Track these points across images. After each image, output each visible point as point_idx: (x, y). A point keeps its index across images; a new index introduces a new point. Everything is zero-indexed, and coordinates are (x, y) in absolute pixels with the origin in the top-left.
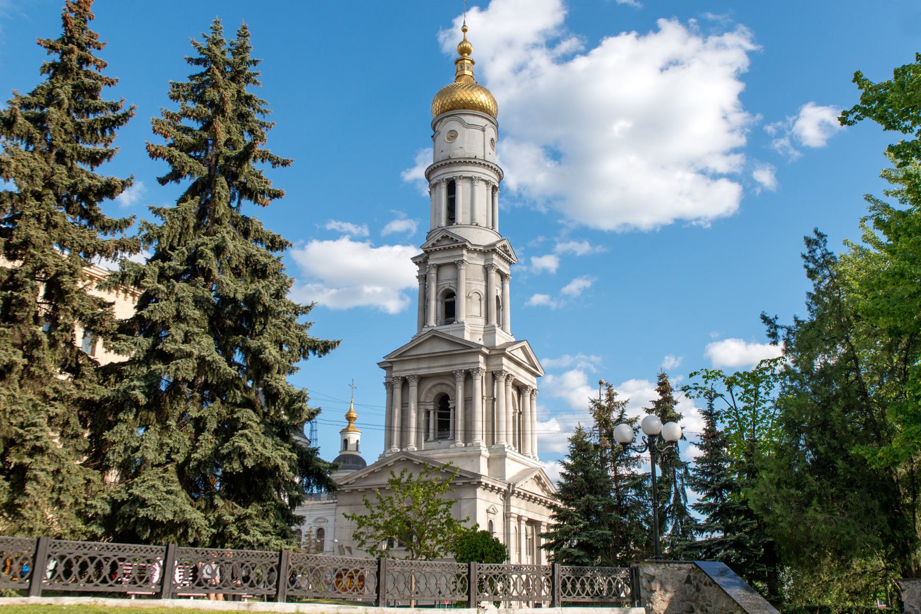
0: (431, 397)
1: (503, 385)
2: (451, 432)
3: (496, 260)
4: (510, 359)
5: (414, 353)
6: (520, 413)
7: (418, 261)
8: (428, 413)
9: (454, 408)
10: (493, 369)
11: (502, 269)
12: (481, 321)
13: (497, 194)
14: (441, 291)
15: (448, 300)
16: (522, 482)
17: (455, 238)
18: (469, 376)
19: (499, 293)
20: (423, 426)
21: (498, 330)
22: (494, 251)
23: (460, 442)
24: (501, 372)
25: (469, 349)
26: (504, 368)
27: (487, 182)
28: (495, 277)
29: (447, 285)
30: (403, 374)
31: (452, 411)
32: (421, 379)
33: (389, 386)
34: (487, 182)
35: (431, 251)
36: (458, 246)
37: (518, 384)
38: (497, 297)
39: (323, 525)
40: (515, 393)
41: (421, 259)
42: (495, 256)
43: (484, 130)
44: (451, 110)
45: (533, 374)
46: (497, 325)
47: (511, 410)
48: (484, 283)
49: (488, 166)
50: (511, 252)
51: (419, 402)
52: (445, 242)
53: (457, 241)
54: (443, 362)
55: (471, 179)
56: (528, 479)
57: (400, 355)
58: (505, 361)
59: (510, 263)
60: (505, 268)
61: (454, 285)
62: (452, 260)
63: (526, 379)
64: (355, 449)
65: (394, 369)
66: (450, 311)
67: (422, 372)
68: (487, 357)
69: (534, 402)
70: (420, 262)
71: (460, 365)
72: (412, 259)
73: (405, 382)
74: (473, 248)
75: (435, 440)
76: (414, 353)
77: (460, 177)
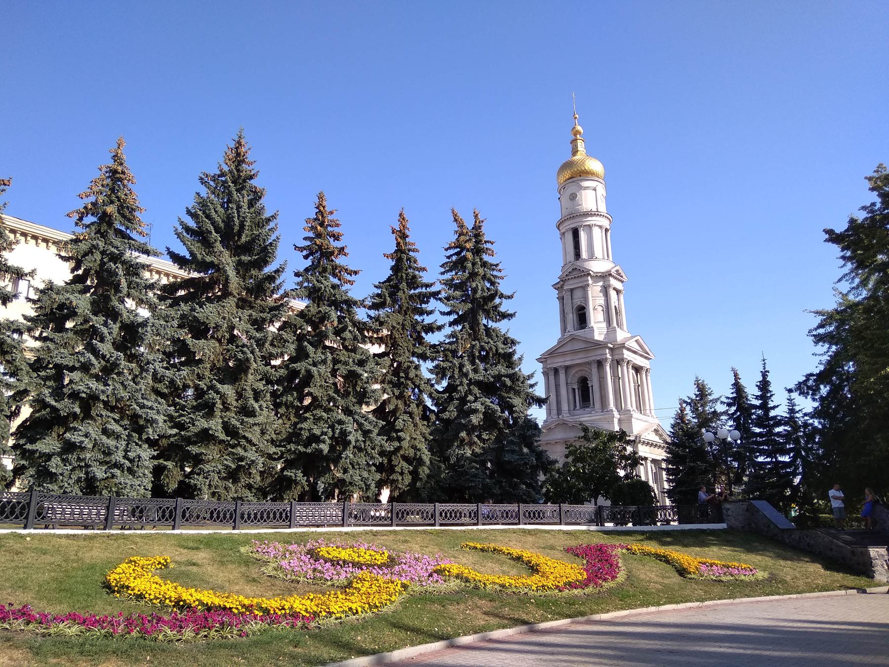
0: (575, 380)
1: (625, 368)
2: (591, 403)
3: (613, 282)
4: (629, 350)
5: (560, 351)
6: (639, 386)
7: (557, 286)
8: (574, 390)
9: (592, 386)
10: (617, 357)
12: (604, 325)
13: (609, 234)
14: (575, 307)
15: (580, 312)
16: (646, 434)
18: (600, 364)
19: (617, 304)
22: (610, 275)
24: (623, 360)
25: (599, 345)
26: (625, 356)
27: (601, 227)
28: (613, 294)
29: (578, 302)
30: (555, 366)
31: (590, 388)
32: (567, 368)
34: (601, 227)
36: (584, 275)
37: (636, 366)
38: (615, 306)
41: (559, 285)
42: (611, 278)
43: (595, 189)
44: (571, 178)
45: (646, 358)
46: (617, 327)
47: (632, 385)
49: (601, 215)
50: (623, 274)
54: (581, 355)
55: (590, 227)
56: (650, 432)
58: (625, 351)
59: (622, 282)
60: (619, 286)
62: (581, 285)
63: (642, 362)
66: (582, 318)
68: (611, 349)
69: (649, 378)
71: (594, 356)
73: (556, 371)
76: (560, 351)
77: (581, 225)
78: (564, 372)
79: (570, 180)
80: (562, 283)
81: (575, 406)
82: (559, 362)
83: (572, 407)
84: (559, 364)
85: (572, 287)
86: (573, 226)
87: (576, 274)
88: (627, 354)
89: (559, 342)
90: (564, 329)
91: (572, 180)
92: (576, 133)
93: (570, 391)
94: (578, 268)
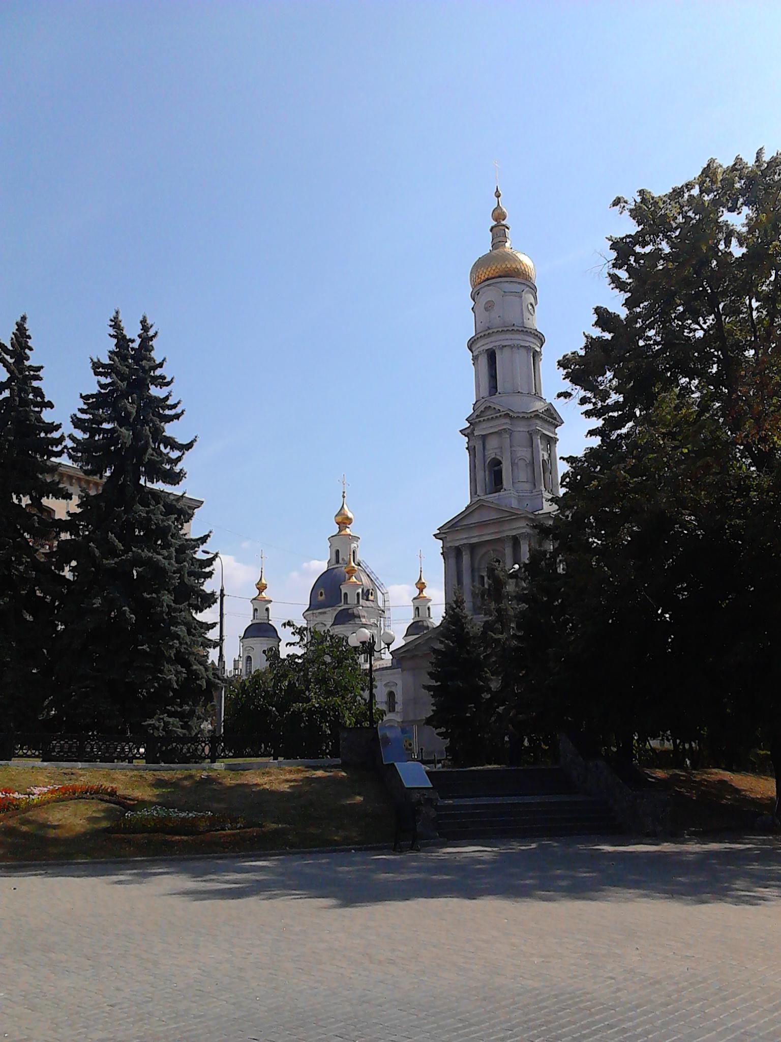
3: (539, 426)
7: (466, 432)
14: (488, 462)
15: (496, 468)
17: (497, 408)
18: (516, 541)
19: (546, 457)
25: (514, 516)
27: (528, 348)
28: (539, 443)
32: (473, 548)
35: (476, 422)
36: (500, 416)
38: (543, 460)
39: (393, 689)
48: (530, 450)
52: (488, 413)
53: (499, 410)
54: (493, 529)
61: (499, 454)
62: (496, 430)
64: (427, 616)
65: (448, 539)
70: (468, 433)
72: (461, 431)
74: (515, 415)
78: (468, 552)
82: (462, 539)
84: (462, 542)
86: (486, 347)
87: (489, 414)
89: (467, 508)
90: (474, 492)
93: (477, 578)
94: (493, 406)
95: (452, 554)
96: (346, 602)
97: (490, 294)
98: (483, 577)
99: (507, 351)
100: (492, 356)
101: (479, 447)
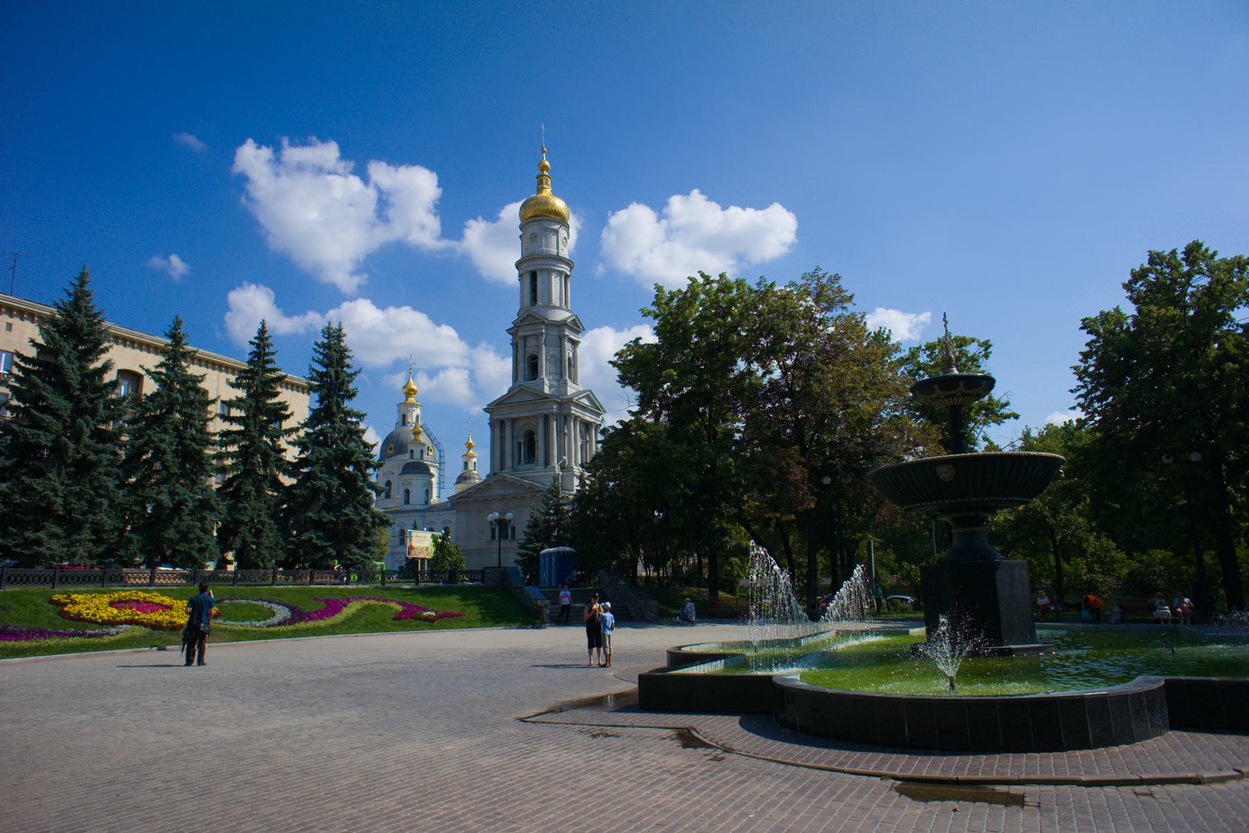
7: (512, 331)
11: (572, 337)
13: (569, 280)
18: (547, 419)
19: (571, 355)
20: (516, 456)
21: (569, 382)
23: (541, 467)
26: (573, 412)
28: (568, 345)
30: (502, 417)
32: (514, 421)
33: (492, 425)
38: (569, 358)
39: (449, 525)
40: (583, 429)
41: (513, 331)
48: (559, 349)
51: (513, 437)
57: (499, 404)
62: (535, 333)
66: (533, 369)
67: (514, 416)
73: (502, 423)
75: (525, 463)
79: (532, 219)
80: (516, 328)
81: (520, 461)
82: (506, 414)
83: (516, 461)
84: (505, 416)
85: (525, 334)
86: (532, 268)
88: (575, 411)
91: (536, 218)
92: (544, 168)
93: (516, 444)
95: (498, 425)
96: (412, 457)
97: (534, 229)
98: (520, 443)
99: (545, 273)
100: (534, 276)
101: (521, 344)
